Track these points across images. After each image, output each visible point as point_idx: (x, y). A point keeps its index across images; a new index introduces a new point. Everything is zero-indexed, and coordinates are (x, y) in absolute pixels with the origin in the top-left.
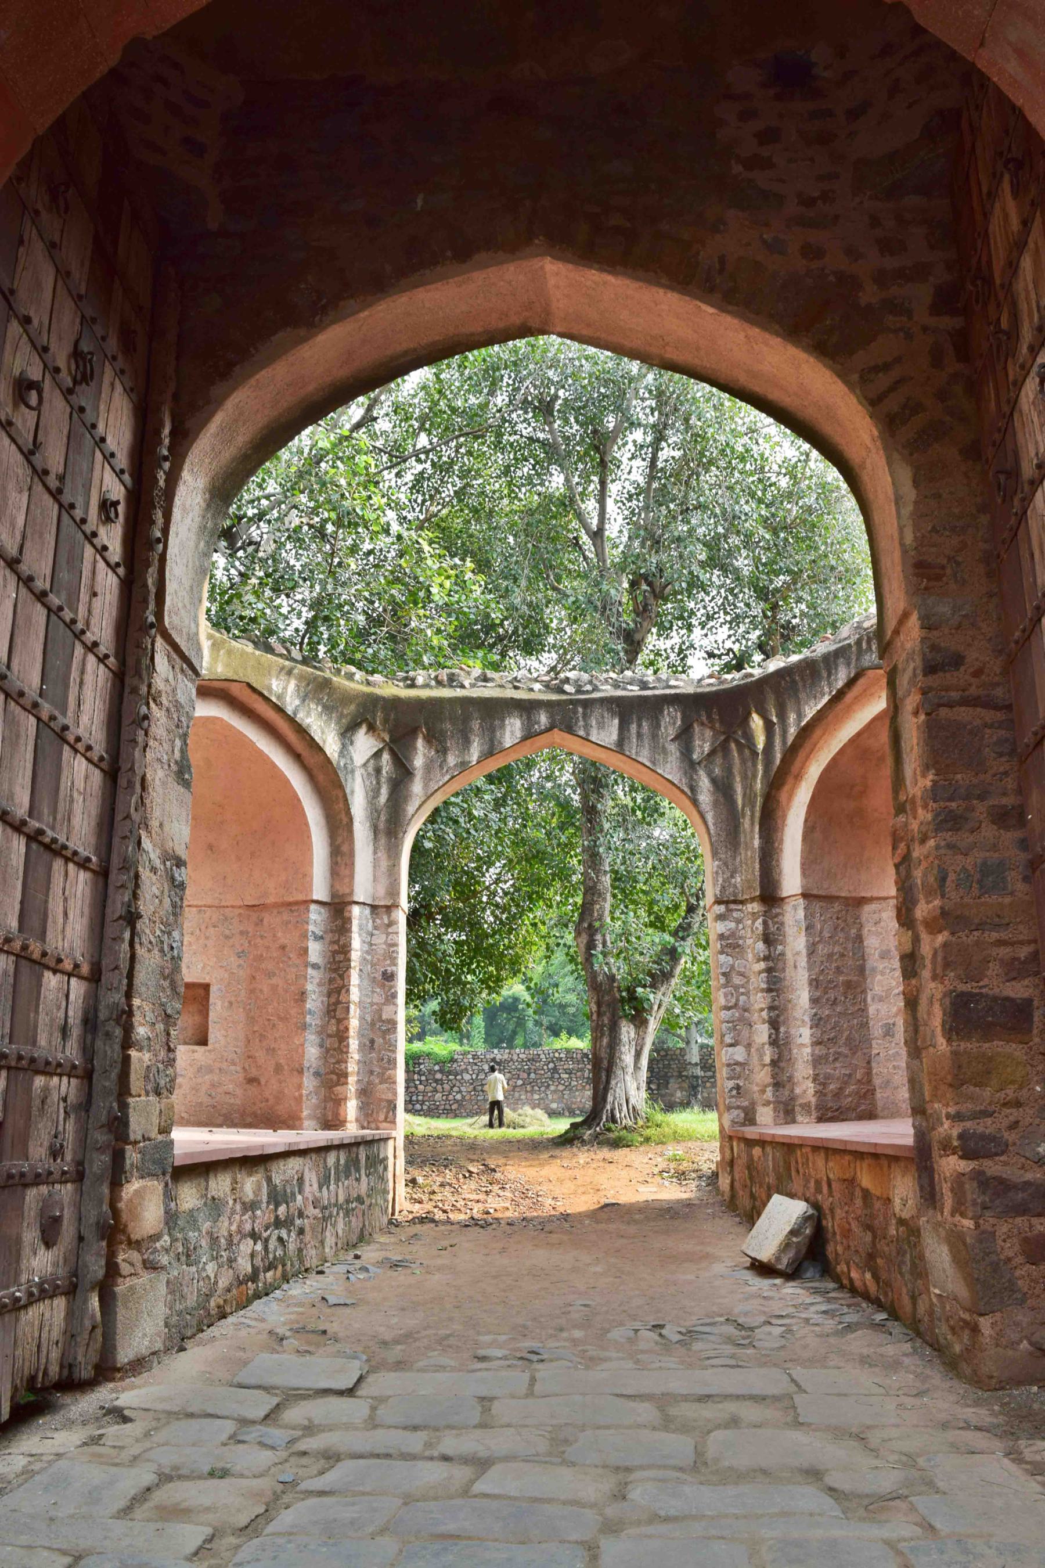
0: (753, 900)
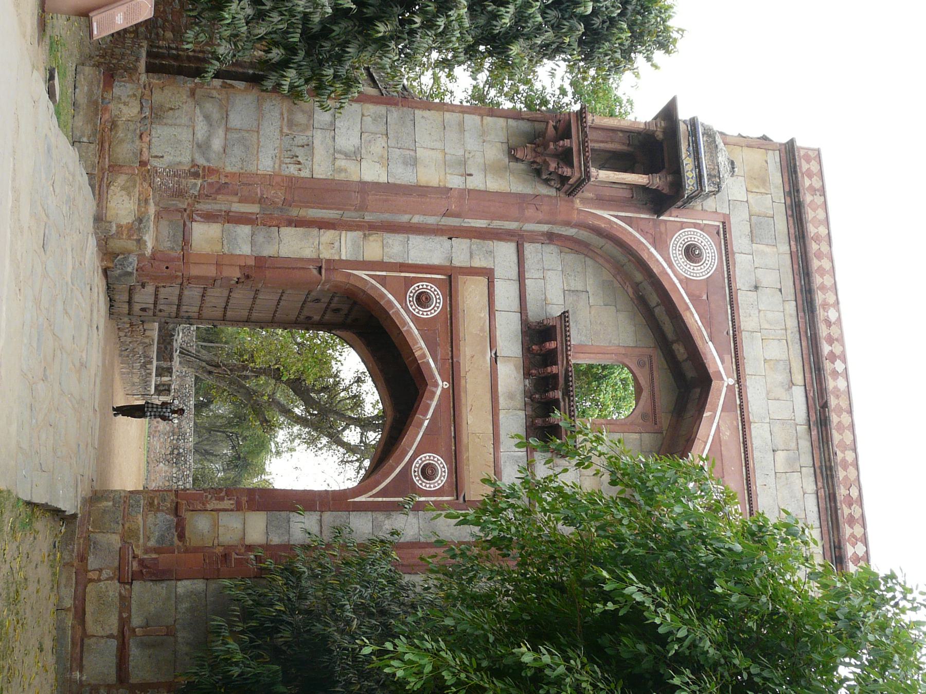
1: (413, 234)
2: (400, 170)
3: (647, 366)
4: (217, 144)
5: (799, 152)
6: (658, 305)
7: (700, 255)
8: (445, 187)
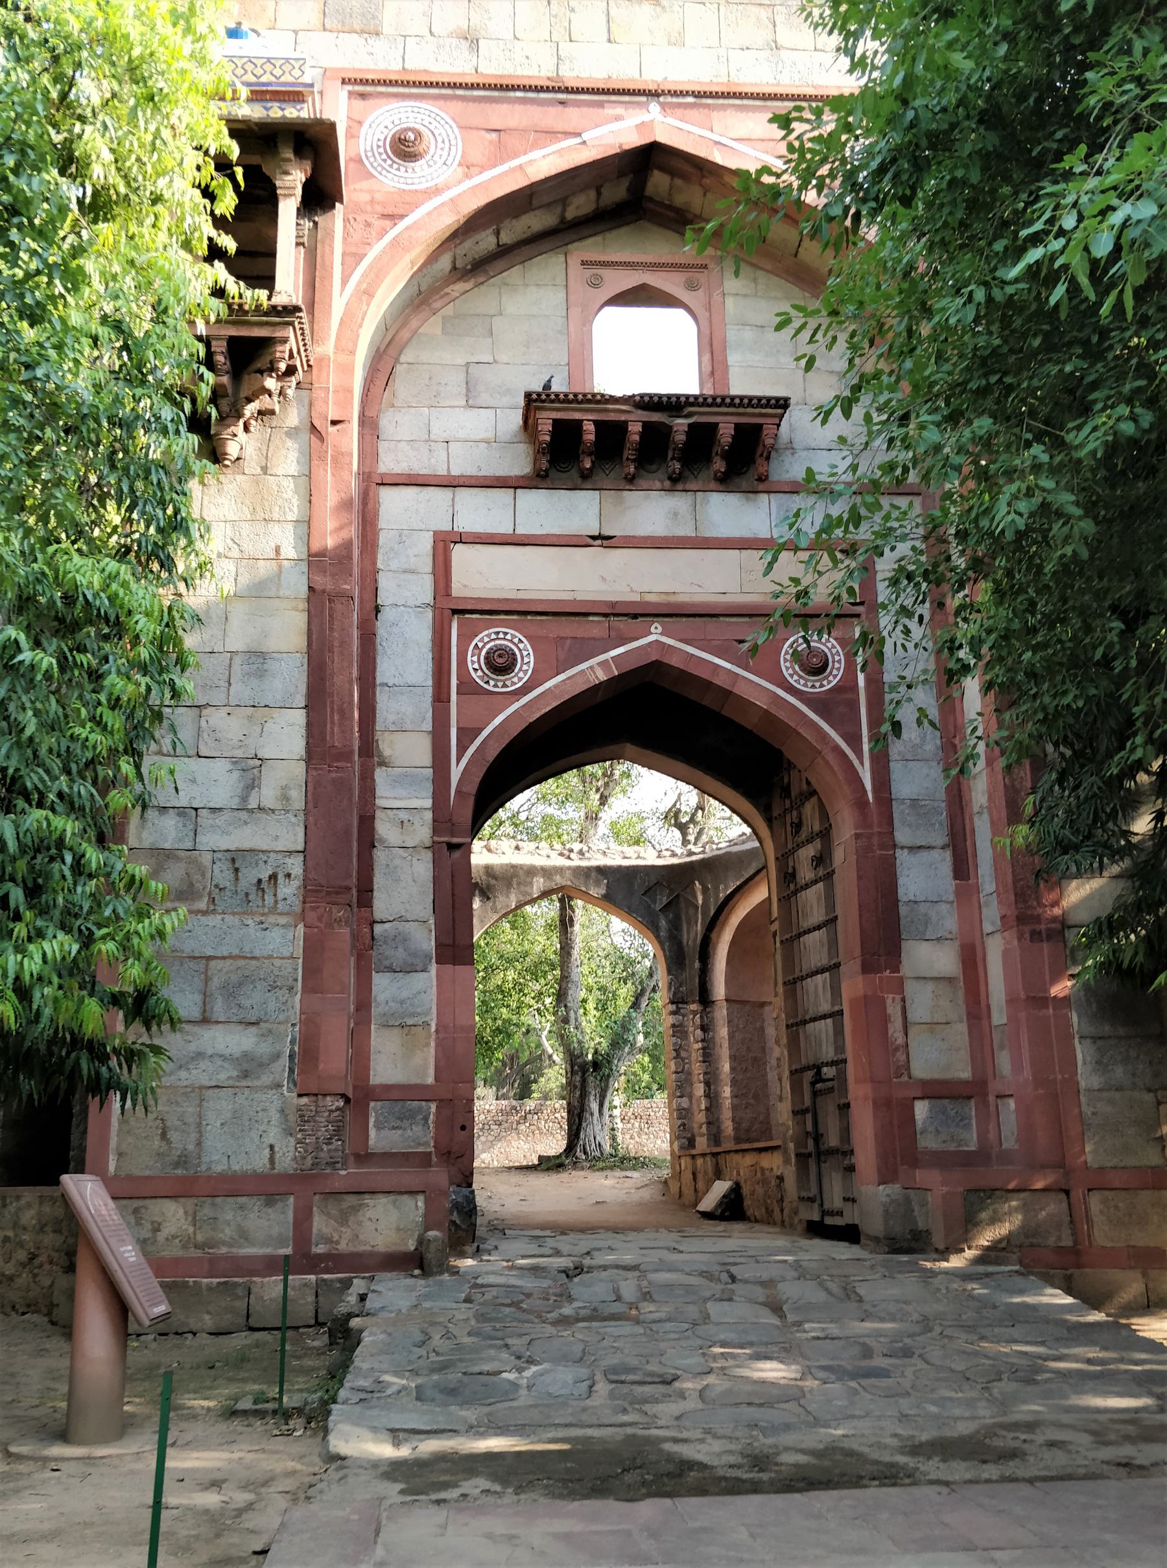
2: (278, 684)
3: (599, 272)
6: (497, 233)
8: (308, 600)
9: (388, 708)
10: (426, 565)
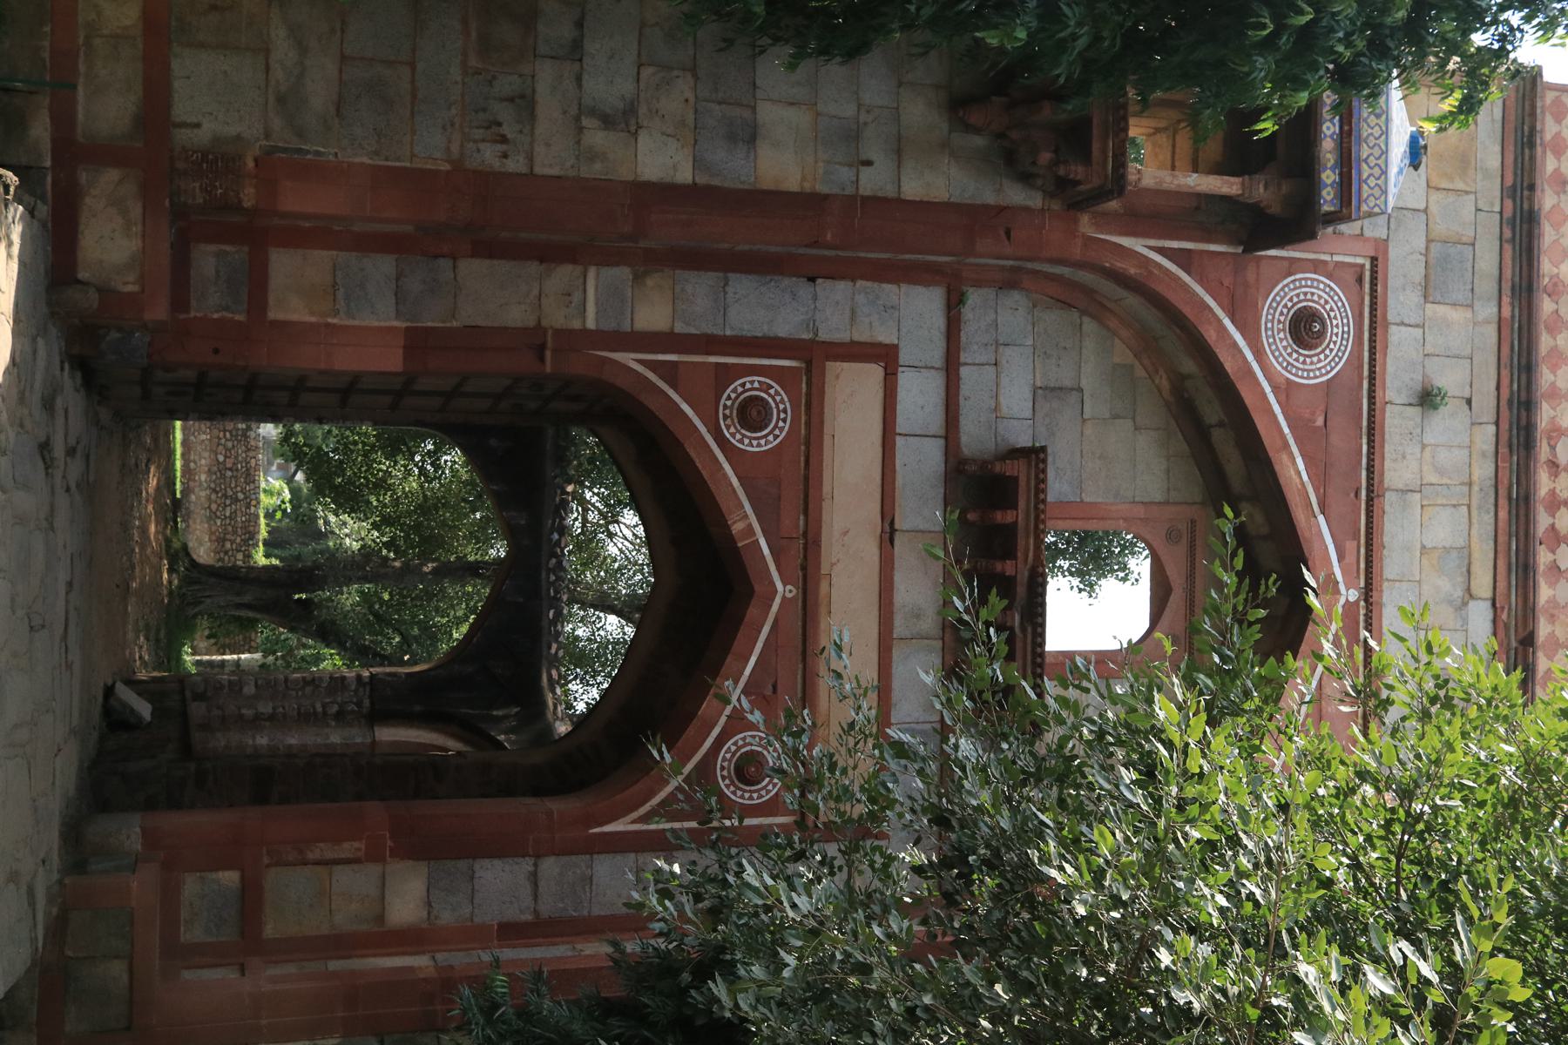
0: (372, 703)
1: (734, 271)
3: (1184, 541)
4: (319, 94)
5: (1543, 97)
6: (1221, 424)
7: (1321, 334)
9: (699, 287)
10: (861, 335)
